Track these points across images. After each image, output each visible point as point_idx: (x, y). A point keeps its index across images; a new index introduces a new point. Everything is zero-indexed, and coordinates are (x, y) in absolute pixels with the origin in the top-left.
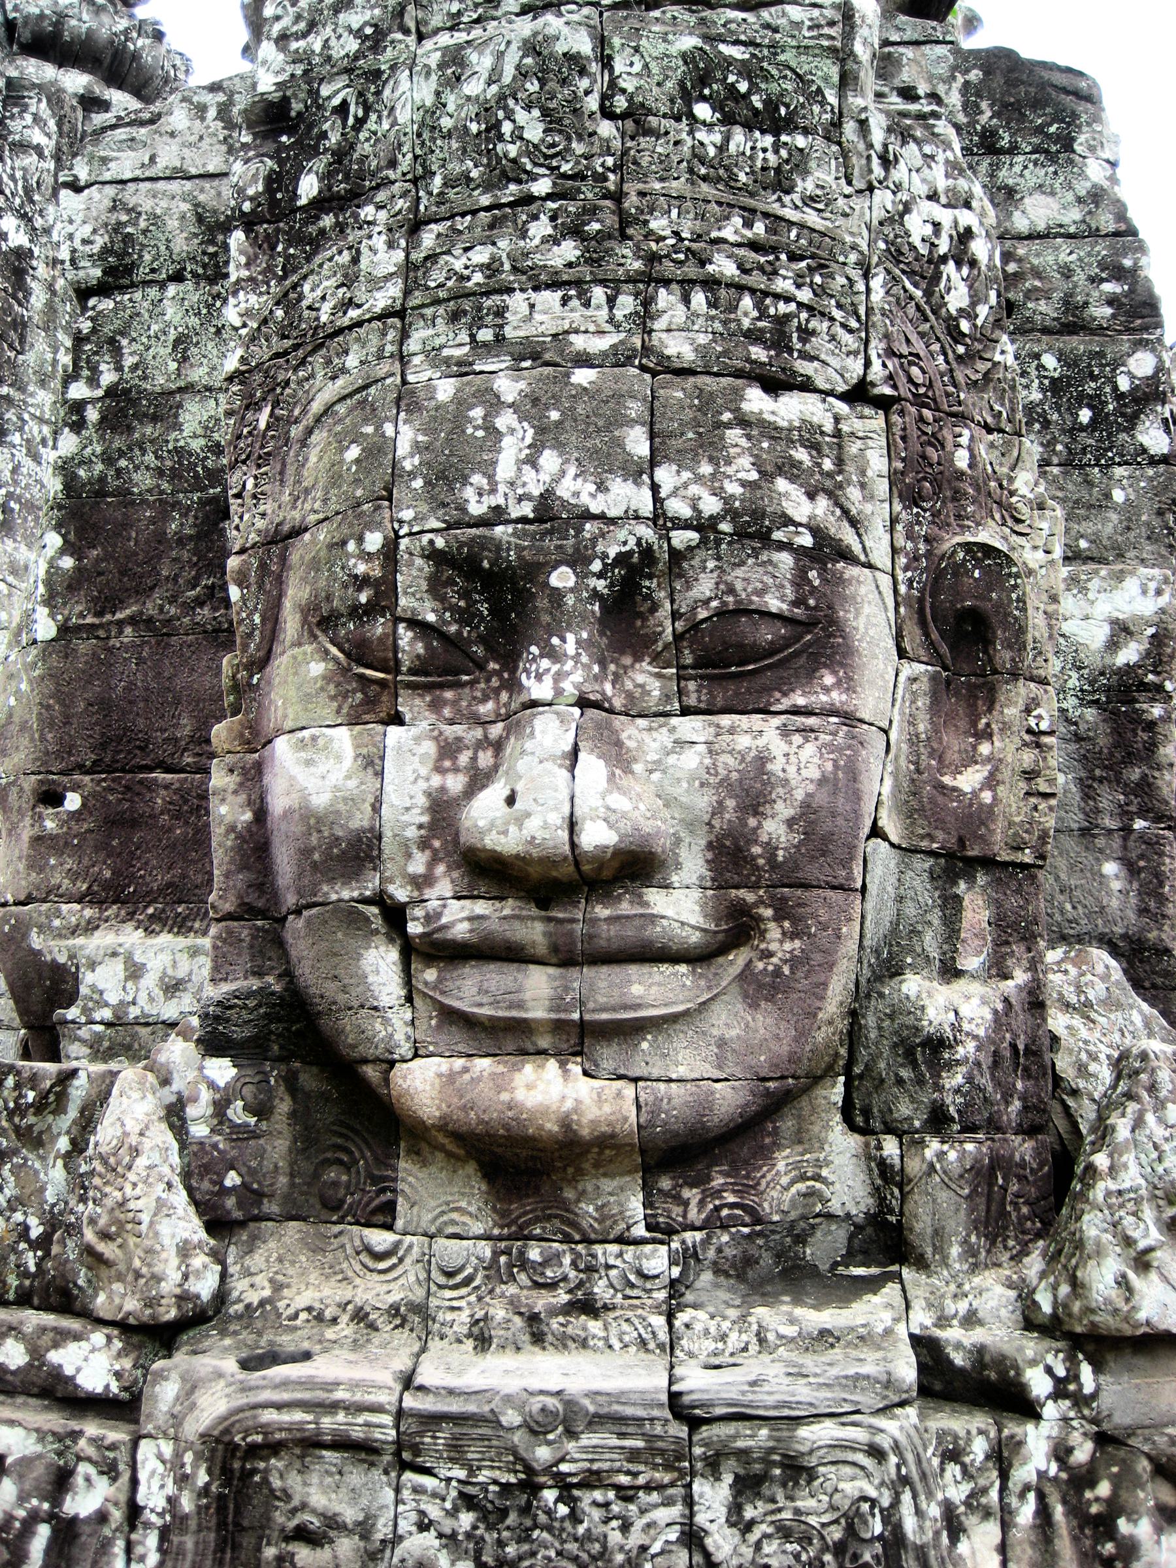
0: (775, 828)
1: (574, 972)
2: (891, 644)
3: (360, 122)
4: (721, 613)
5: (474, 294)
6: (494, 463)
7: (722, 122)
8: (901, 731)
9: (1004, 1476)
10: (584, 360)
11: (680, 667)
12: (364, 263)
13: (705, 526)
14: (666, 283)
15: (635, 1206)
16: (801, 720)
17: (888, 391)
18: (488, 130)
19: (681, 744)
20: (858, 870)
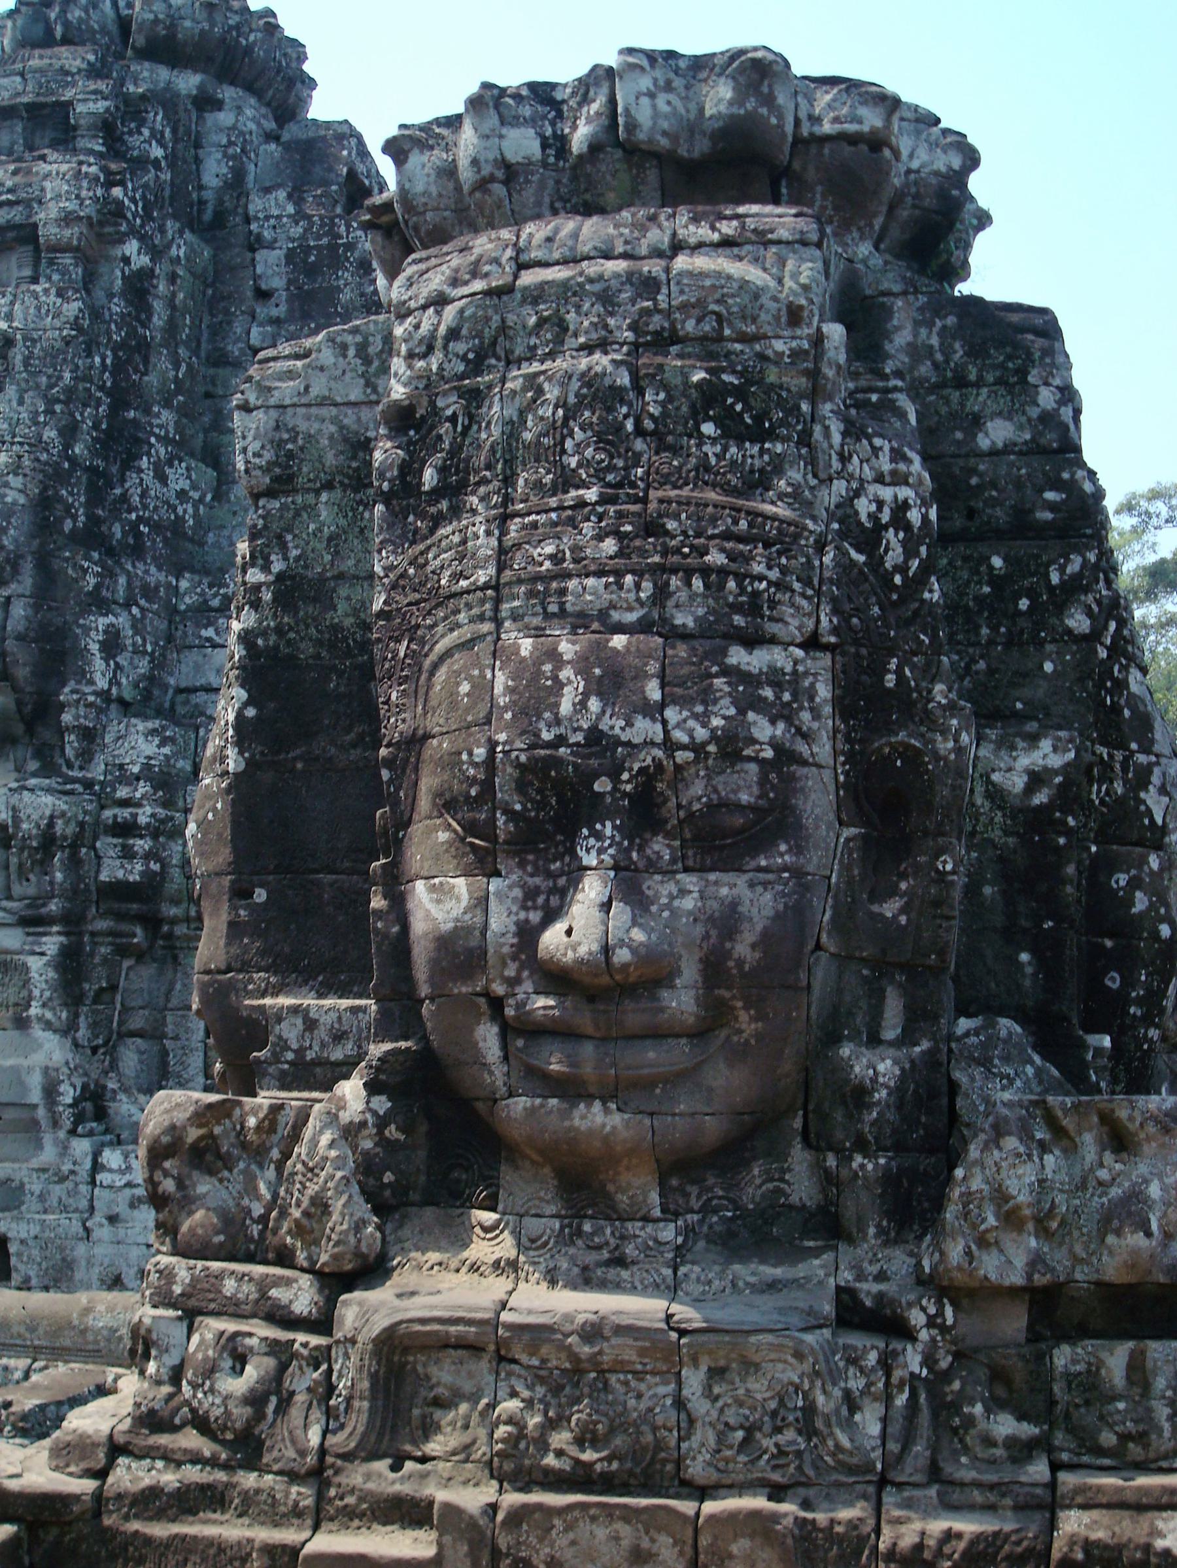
0: (743, 948)
2: (832, 816)
3: (466, 429)
4: (709, 805)
6: (557, 705)
7: (722, 437)
8: (839, 876)
9: (888, 1375)
10: (620, 629)
11: (683, 840)
13: (698, 749)
14: (674, 571)
15: (654, 1197)
16: (762, 876)
17: (833, 639)
19: (683, 892)
20: (803, 976)
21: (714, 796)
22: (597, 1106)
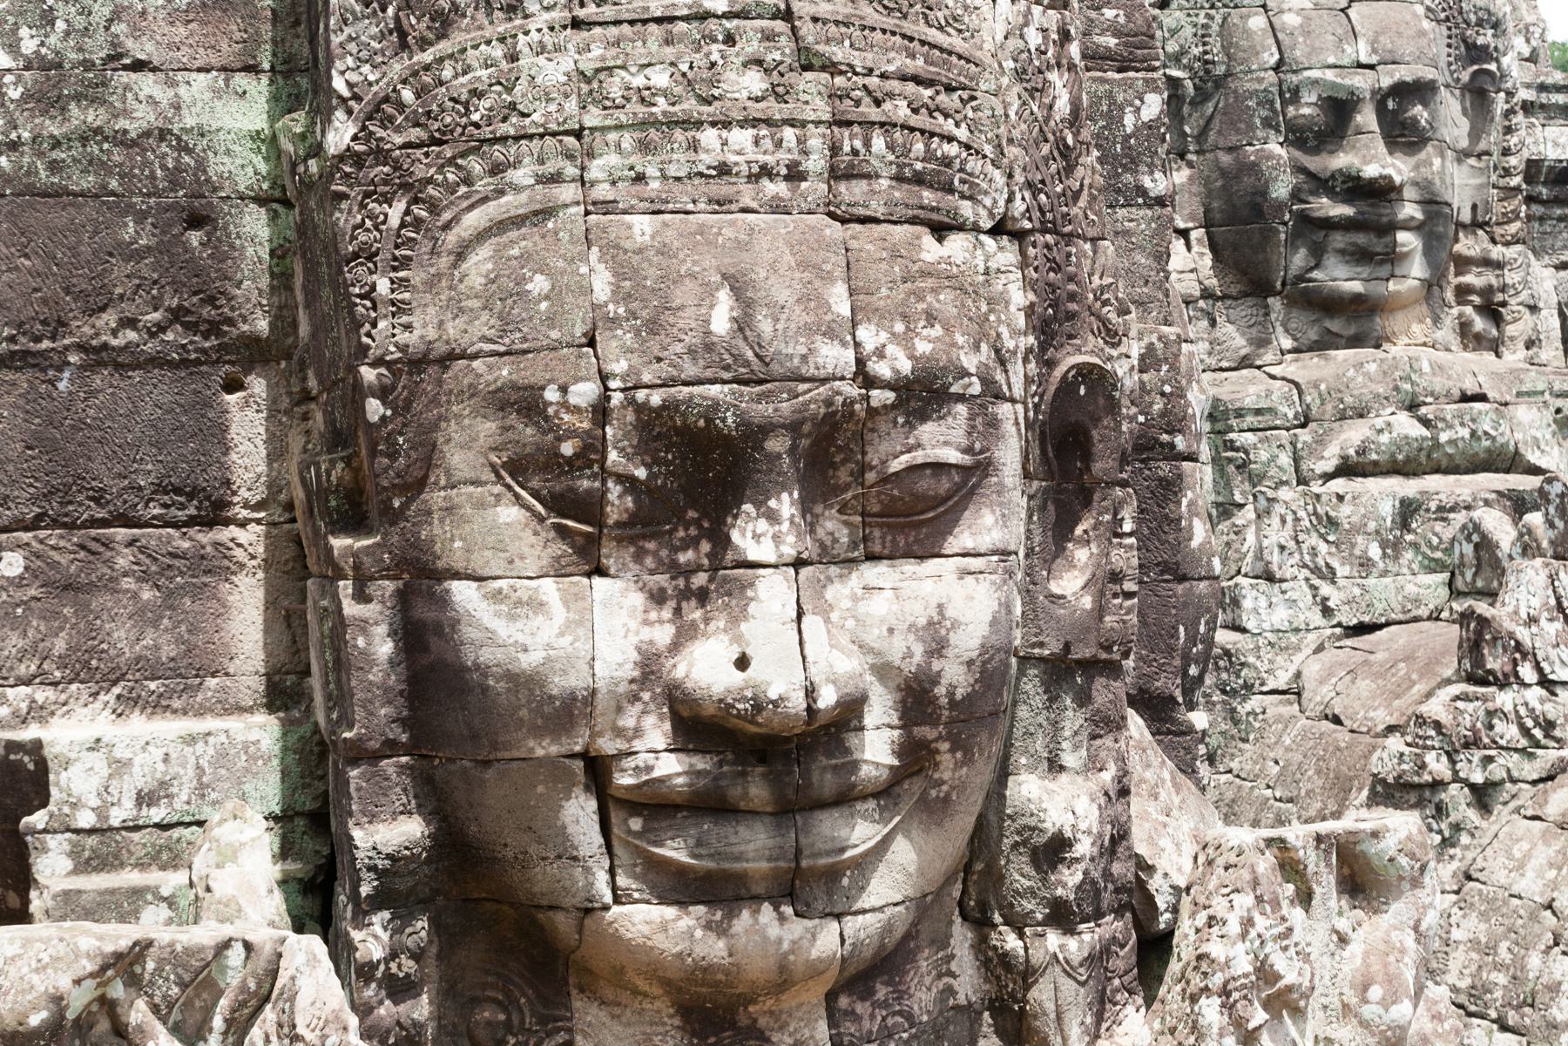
22: (767, 908)
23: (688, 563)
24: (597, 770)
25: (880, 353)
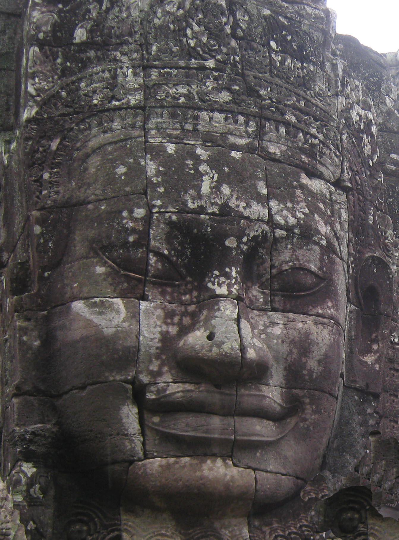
1: (231, 420)
4: (293, 268)
5: (182, 107)
12: (120, 79)
13: (289, 229)
14: (268, 120)
18: (179, 30)
19: (273, 324)
21: (297, 263)
23: (186, 301)
24: (138, 394)
25: (279, 212)
